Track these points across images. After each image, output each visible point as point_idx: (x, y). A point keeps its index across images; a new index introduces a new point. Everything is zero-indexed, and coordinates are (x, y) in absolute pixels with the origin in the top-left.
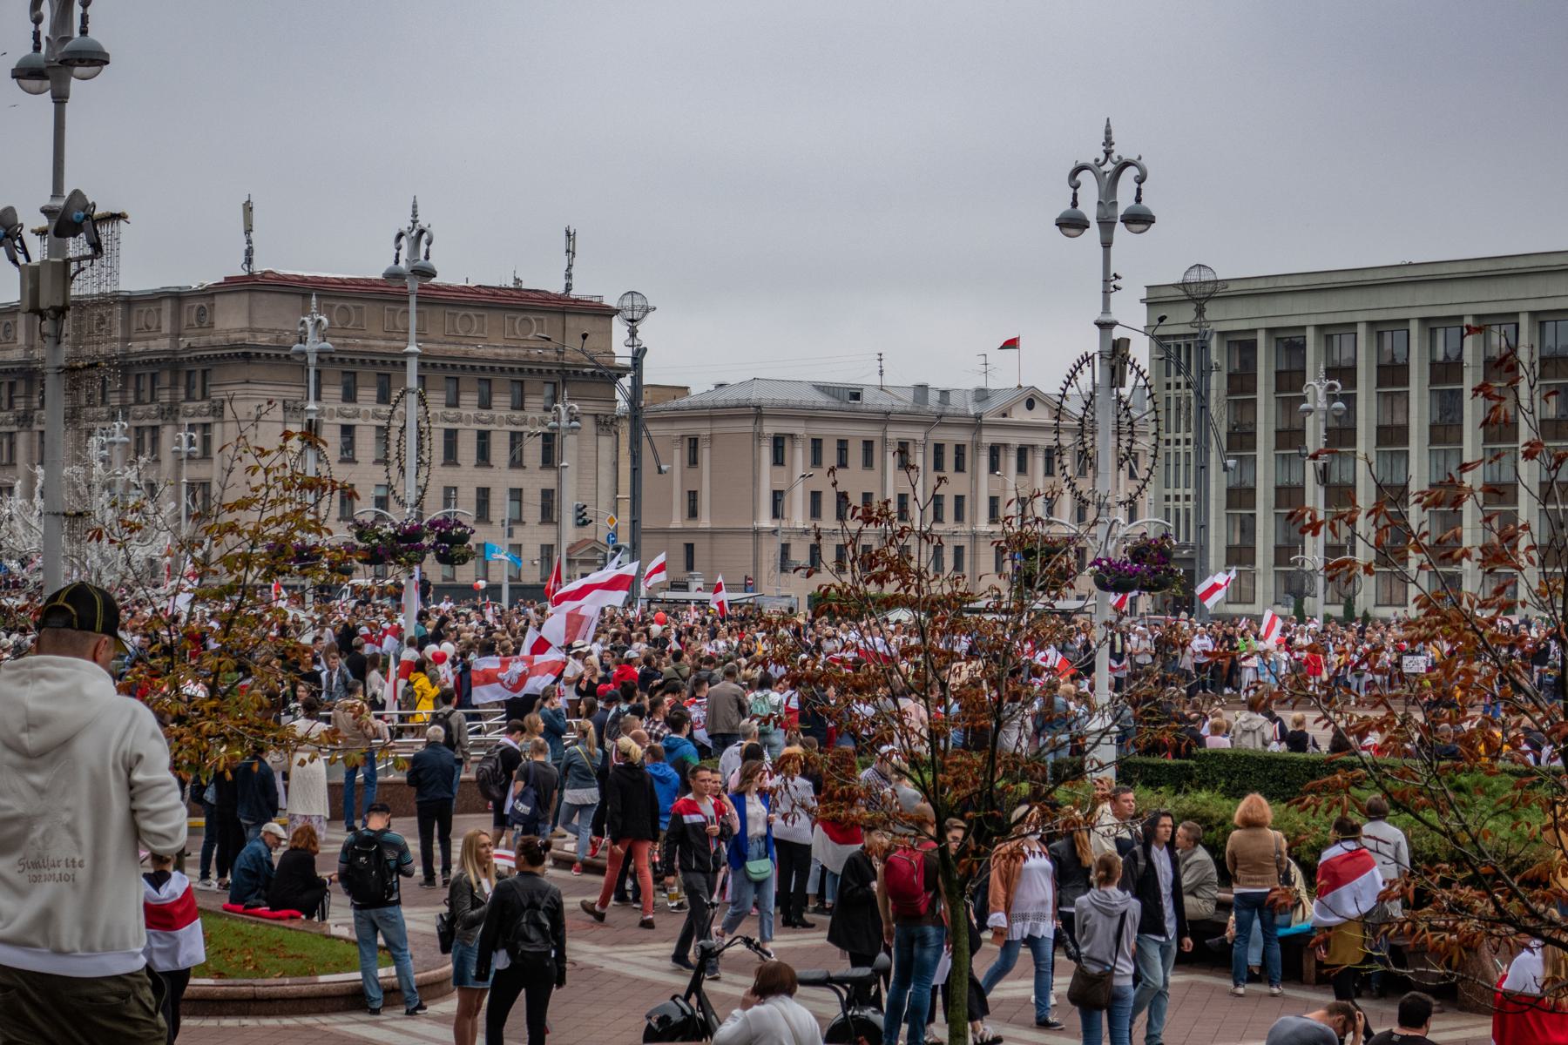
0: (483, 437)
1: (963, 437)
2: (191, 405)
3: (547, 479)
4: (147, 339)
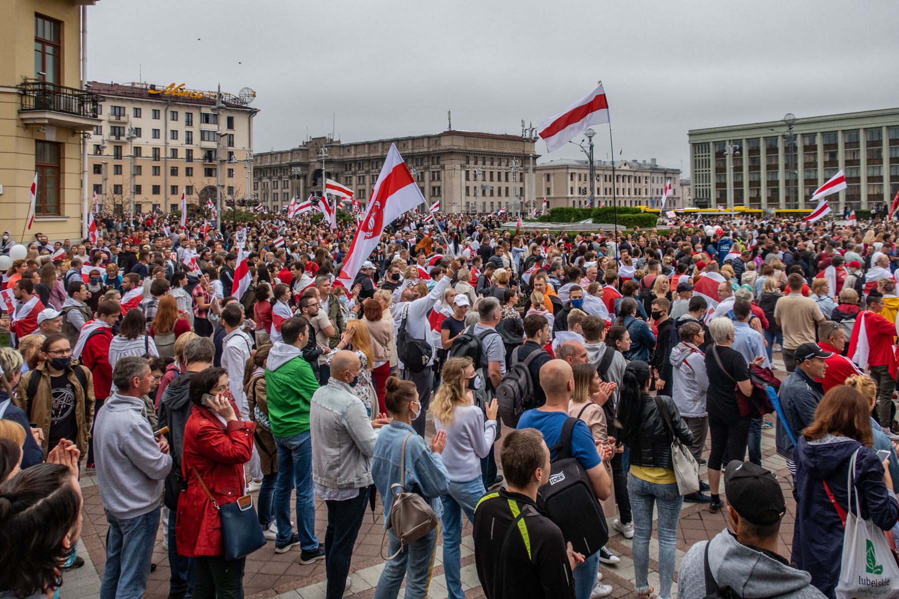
0: (499, 173)
1: (611, 173)
3: (521, 185)
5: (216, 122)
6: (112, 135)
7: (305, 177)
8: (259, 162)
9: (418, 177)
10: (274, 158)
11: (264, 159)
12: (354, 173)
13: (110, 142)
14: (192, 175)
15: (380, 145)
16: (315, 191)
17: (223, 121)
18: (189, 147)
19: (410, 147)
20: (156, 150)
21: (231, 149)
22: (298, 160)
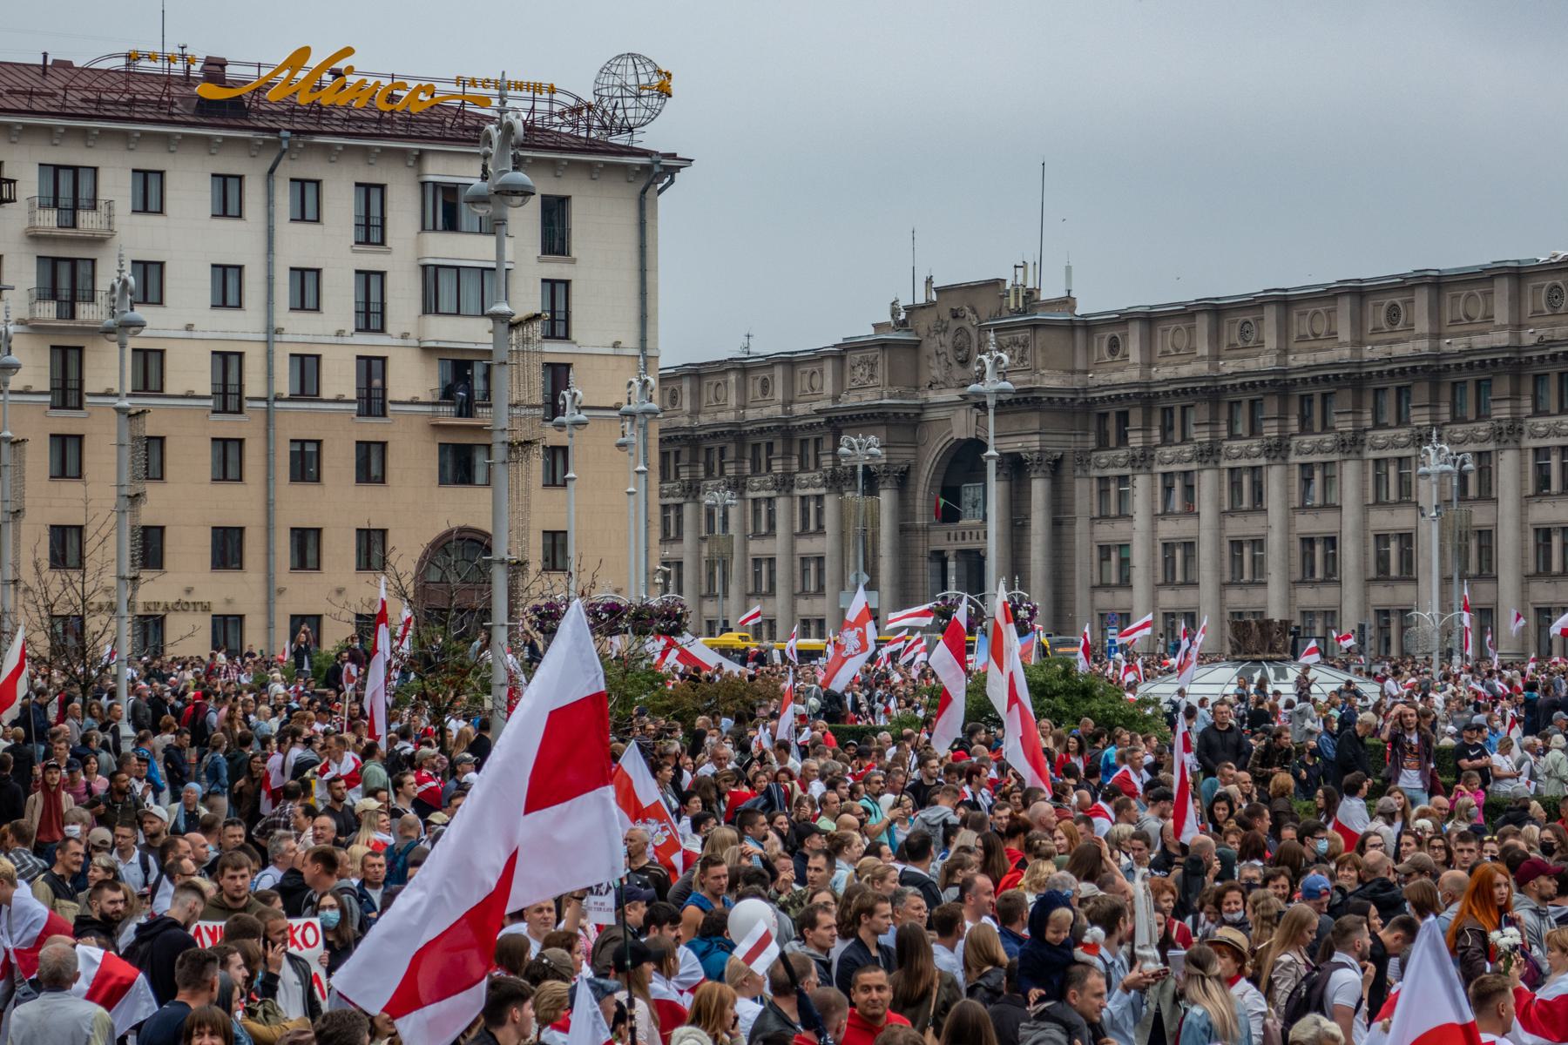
2: (1542, 421)
4: (1468, 334)
5: (494, 227)
6: (41, 298)
7: (903, 480)
8: (687, 406)
9: (1463, 477)
10: (754, 389)
11: (708, 394)
12: (1143, 460)
13: (36, 329)
14: (382, 480)
15: (1270, 315)
16: (951, 548)
17: (525, 221)
18: (371, 344)
19: (1423, 325)
20: (227, 362)
21: (555, 350)
22: (869, 398)
